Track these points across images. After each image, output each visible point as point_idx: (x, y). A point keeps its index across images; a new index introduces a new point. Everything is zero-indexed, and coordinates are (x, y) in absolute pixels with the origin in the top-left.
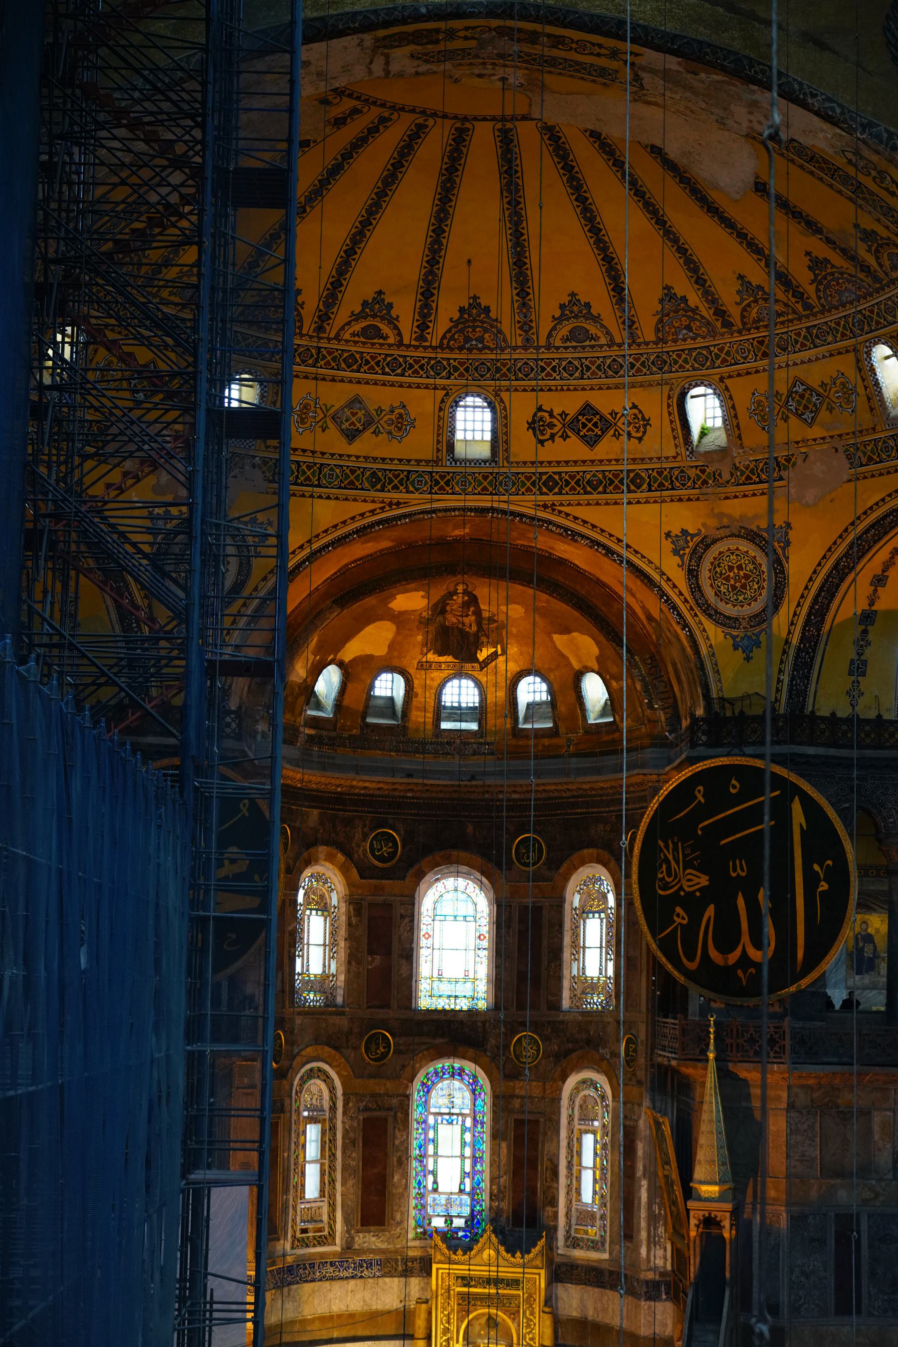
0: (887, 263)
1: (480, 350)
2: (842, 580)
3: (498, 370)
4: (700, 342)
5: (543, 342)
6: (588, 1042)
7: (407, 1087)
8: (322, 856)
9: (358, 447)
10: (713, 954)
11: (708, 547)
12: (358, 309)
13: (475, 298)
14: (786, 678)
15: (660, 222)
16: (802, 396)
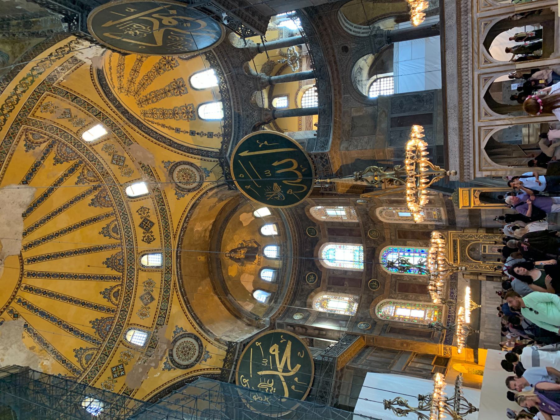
0: (41, 140)
1: (123, 260)
2: (176, 143)
3: (131, 254)
4: (109, 193)
5: (119, 241)
6: (367, 214)
7: (389, 275)
8: (310, 301)
9: (156, 296)
10: (299, 180)
11: (179, 186)
12: (106, 299)
13: (103, 263)
14: (213, 159)
15: (60, 210)
16: (117, 161)
